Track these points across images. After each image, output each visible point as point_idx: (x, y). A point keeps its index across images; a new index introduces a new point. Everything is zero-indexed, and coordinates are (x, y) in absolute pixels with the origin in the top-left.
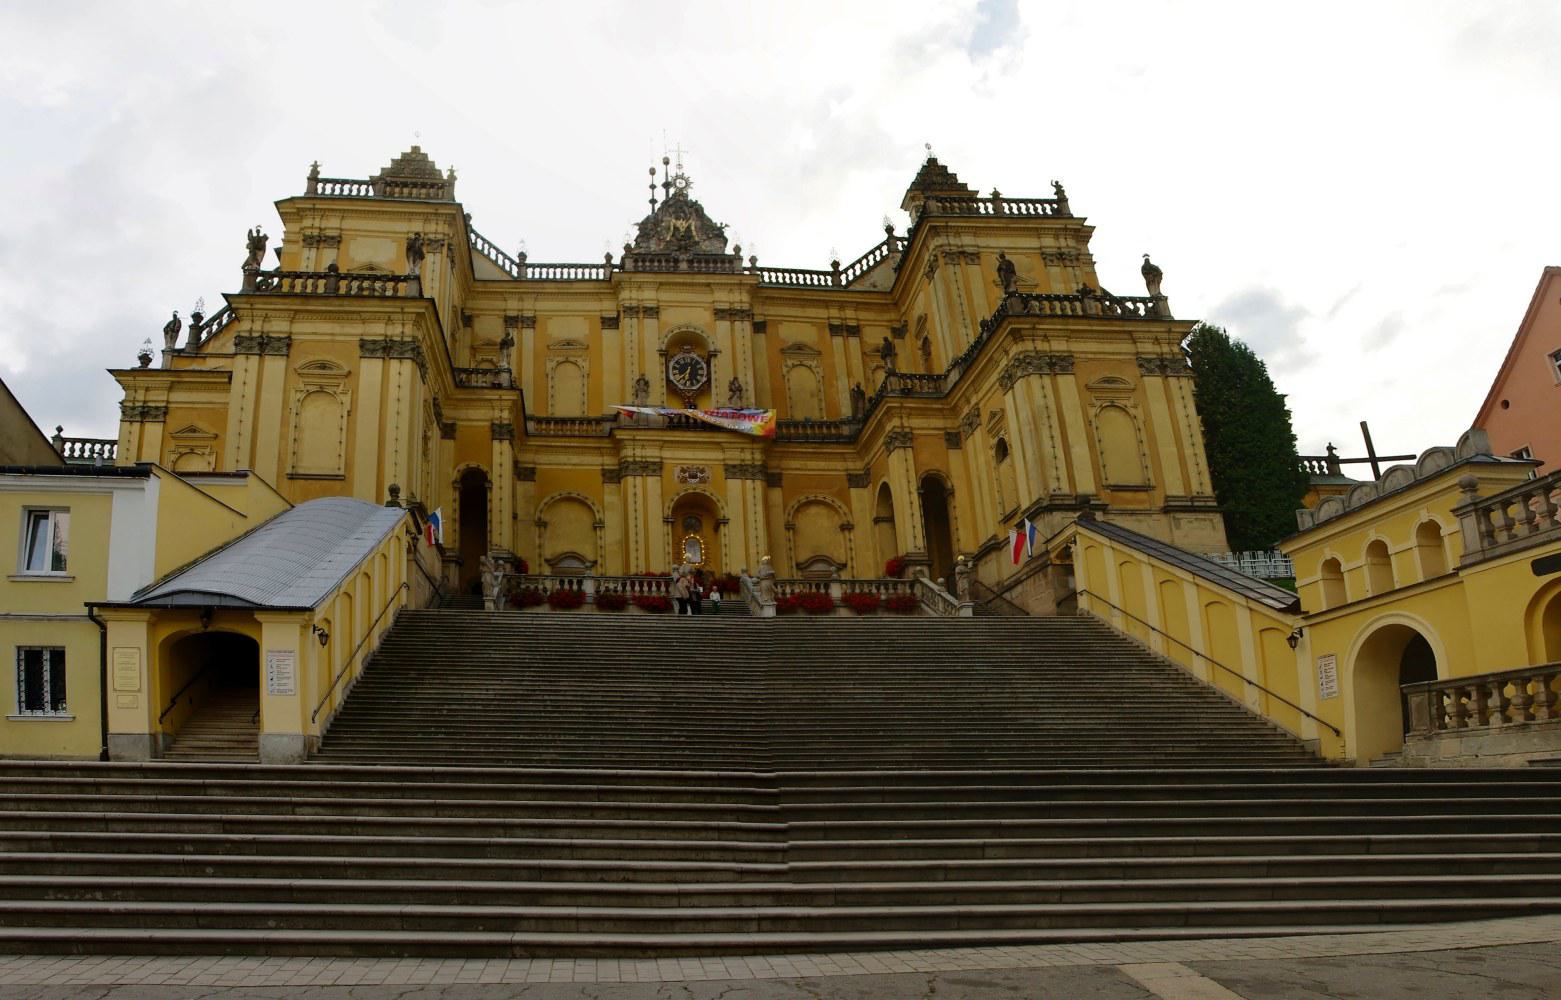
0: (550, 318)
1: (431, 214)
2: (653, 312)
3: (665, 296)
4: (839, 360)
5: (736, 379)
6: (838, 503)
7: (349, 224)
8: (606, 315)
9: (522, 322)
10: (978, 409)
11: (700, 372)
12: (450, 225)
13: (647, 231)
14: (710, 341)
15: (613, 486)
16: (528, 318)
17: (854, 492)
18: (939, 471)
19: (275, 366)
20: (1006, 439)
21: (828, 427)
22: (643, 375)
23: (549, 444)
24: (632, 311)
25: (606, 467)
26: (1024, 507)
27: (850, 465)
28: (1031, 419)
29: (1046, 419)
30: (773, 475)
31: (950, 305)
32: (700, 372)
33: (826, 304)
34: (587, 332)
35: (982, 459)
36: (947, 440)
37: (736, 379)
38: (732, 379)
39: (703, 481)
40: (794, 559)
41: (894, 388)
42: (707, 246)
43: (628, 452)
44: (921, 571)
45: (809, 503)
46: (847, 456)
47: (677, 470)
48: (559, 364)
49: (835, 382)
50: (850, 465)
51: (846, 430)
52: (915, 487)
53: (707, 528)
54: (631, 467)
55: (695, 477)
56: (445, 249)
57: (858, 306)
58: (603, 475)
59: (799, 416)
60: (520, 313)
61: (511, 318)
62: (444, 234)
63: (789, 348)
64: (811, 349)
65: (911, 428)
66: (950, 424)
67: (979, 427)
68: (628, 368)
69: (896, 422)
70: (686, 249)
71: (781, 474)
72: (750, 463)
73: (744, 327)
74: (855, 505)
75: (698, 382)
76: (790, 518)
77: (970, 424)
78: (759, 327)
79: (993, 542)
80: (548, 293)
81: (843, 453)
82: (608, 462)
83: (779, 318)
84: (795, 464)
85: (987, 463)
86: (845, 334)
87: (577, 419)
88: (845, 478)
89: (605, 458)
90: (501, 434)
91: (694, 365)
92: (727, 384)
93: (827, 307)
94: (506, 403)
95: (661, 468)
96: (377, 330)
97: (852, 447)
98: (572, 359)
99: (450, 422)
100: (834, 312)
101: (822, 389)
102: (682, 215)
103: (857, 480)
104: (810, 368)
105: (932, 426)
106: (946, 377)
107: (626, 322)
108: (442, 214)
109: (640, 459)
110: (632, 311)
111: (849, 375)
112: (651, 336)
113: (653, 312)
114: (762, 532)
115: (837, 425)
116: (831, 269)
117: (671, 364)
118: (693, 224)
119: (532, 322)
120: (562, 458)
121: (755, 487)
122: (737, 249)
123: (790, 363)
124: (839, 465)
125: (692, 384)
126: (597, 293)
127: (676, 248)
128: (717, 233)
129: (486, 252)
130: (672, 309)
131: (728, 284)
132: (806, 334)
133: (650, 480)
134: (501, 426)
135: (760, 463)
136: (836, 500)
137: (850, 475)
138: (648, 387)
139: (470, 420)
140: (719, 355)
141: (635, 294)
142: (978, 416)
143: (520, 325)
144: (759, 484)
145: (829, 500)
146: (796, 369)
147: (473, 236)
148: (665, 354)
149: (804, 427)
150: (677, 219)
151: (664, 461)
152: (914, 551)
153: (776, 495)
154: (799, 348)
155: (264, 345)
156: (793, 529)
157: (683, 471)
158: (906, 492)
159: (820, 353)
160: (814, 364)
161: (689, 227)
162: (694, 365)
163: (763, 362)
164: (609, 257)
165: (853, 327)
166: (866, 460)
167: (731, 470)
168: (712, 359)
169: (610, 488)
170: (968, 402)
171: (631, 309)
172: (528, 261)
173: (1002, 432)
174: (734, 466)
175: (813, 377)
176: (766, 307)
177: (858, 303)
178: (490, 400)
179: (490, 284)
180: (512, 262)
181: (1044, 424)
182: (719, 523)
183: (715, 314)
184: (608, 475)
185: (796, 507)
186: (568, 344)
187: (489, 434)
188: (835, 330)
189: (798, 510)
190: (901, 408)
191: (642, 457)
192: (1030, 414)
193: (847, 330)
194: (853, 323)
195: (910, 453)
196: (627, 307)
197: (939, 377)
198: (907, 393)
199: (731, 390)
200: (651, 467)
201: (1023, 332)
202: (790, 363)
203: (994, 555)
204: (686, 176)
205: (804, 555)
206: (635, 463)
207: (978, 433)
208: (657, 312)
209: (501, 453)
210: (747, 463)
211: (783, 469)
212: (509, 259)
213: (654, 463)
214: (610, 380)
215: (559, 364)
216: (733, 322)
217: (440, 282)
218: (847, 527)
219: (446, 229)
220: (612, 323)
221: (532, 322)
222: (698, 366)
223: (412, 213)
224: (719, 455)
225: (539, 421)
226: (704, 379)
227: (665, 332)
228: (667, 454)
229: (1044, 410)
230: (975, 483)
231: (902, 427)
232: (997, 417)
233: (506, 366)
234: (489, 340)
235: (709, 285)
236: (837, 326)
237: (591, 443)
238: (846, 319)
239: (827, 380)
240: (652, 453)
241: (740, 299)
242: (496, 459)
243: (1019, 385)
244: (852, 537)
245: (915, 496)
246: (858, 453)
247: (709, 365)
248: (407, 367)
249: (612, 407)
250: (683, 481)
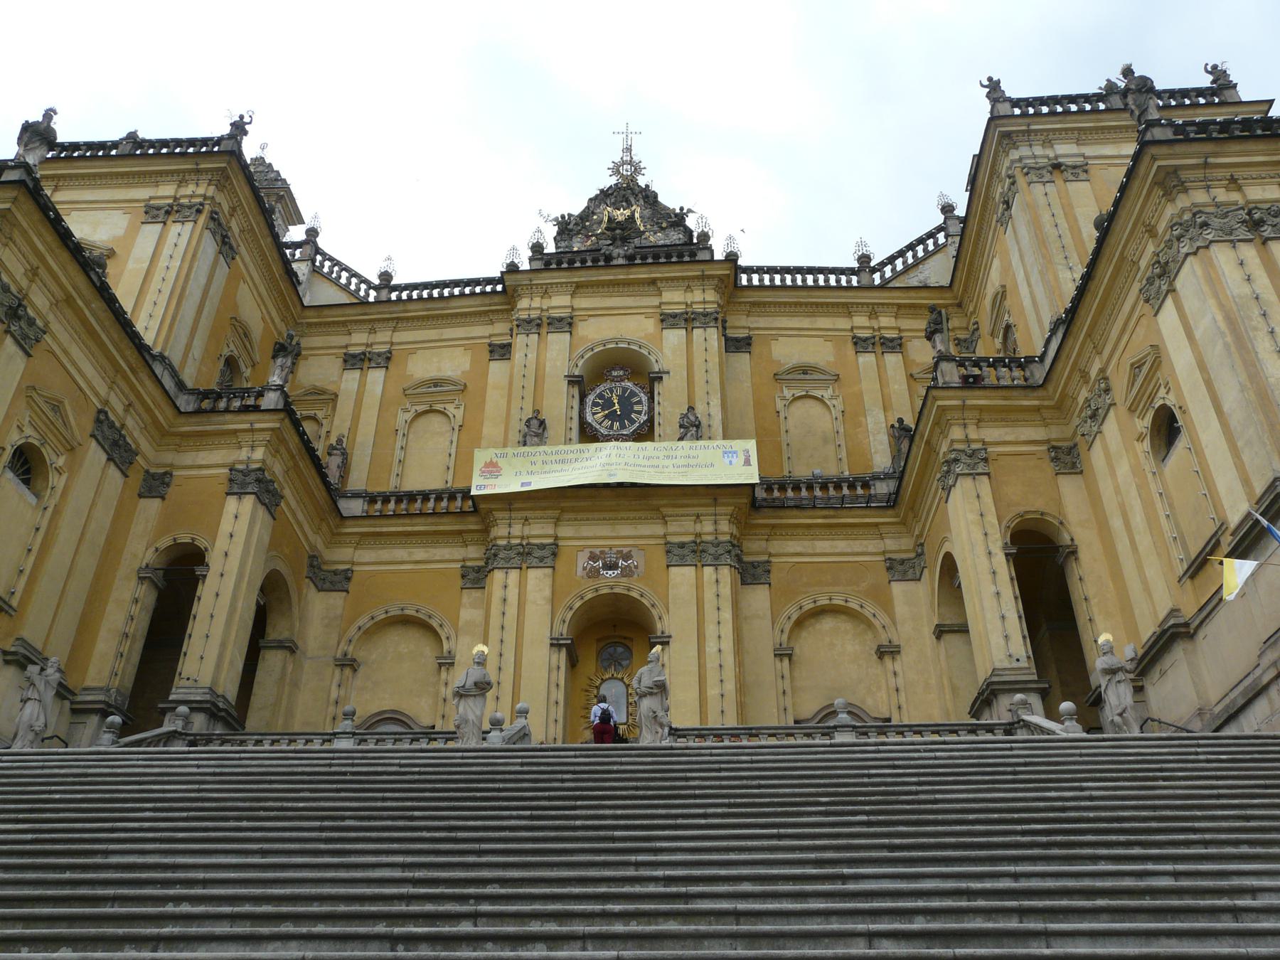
0: (413, 352)
1: (190, 171)
4: (869, 387)
5: (691, 409)
6: (869, 610)
8: (497, 341)
9: (370, 360)
10: (1106, 379)
11: (636, 408)
12: (220, 188)
13: (571, 227)
14: (653, 359)
15: (476, 594)
16: (379, 355)
17: (898, 589)
18: (1042, 514)
20: (1171, 401)
21: (852, 486)
22: (538, 412)
23: (378, 530)
25: (469, 564)
26: (1234, 519)
27: (890, 544)
28: (1222, 325)
29: (1261, 319)
30: (754, 565)
31: (1041, 241)
32: (636, 408)
33: (847, 310)
34: (467, 366)
35: (1123, 469)
36: (1053, 460)
37: (691, 409)
38: (685, 412)
39: (627, 572)
40: (790, 710)
41: (947, 379)
42: (656, 238)
43: (500, 531)
44: (1024, 703)
45: (819, 612)
46: (884, 529)
47: (582, 560)
48: (419, 415)
49: (863, 419)
50: (890, 544)
51: (882, 488)
52: (1000, 544)
54: (502, 555)
55: (613, 566)
56: (202, 219)
57: (900, 310)
58: (463, 576)
60: (368, 349)
61: (354, 356)
62: (205, 197)
63: (789, 371)
64: (823, 372)
65: (984, 443)
66: (1054, 433)
67: (1112, 413)
68: (516, 404)
69: (956, 433)
70: (625, 240)
71: (769, 562)
72: (709, 538)
73: (709, 339)
74: (901, 609)
75: (632, 422)
76: (785, 636)
77: (1093, 416)
78: (736, 345)
79: (1172, 622)
80: (413, 318)
81: (876, 525)
82: (471, 556)
83: (773, 332)
84: (793, 546)
85: (1137, 471)
86: (879, 349)
87: (431, 492)
88: (883, 566)
89: (471, 548)
90: (244, 485)
92: (677, 419)
93: (850, 315)
94: (259, 436)
95: (554, 554)
97: (890, 512)
98: (439, 407)
99: (161, 471)
100: (861, 320)
101: (841, 430)
102: (624, 204)
103: (900, 568)
104: (820, 400)
105: (1023, 438)
106: (1042, 358)
107: (520, 341)
108: (207, 171)
109: (518, 541)
110: (534, 325)
111: (885, 409)
113: (566, 324)
114: (729, 660)
116: (855, 265)
117: (590, 398)
120: (400, 553)
121: (719, 579)
122: (704, 237)
123: (788, 393)
124: (872, 545)
125: (623, 427)
126: (486, 313)
127: (610, 242)
128: (677, 220)
129: (334, 275)
130: (592, 320)
131: (683, 278)
132: (817, 352)
133: (532, 574)
134: (245, 473)
135: (727, 538)
136: (866, 604)
137: (890, 559)
138: (544, 429)
139: (201, 467)
140: (664, 376)
141: (537, 302)
142: (1107, 391)
143: (366, 364)
144: (725, 573)
145: (853, 605)
146: (799, 404)
147: (319, 258)
148: (580, 384)
149: (810, 487)
151: (561, 543)
152: (1006, 664)
154: (805, 370)
156: (790, 656)
157: (593, 558)
158: (981, 550)
159: (837, 378)
160: (827, 394)
161: (632, 217)
162: (626, 401)
163: (743, 391)
165: (892, 340)
166: (917, 533)
167: (677, 551)
168: (656, 384)
169: (469, 597)
170: (1085, 375)
171: (529, 321)
172: (393, 283)
173: (1162, 392)
174: (682, 545)
175: (827, 413)
176: (751, 319)
177: (899, 306)
178: (235, 432)
179: (326, 312)
180: (370, 286)
181: (1255, 329)
183: (662, 321)
184: (472, 576)
185: (794, 617)
186: (435, 386)
187: (225, 488)
188: (861, 344)
189: (799, 624)
190: (963, 407)
191: (522, 538)
192: (1219, 318)
193: (882, 344)
195: (984, 485)
196: (524, 320)
197: (1030, 360)
198: (971, 383)
199: (681, 426)
200: (538, 553)
201: (1184, 175)
202: (788, 393)
203: (1179, 652)
204: (636, 159)
206: (509, 547)
207: (1111, 427)
208: (570, 324)
209: (236, 517)
210: (706, 538)
211: (770, 555)
212: (366, 281)
213: (542, 547)
215: (419, 415)
216: (689, 332)
217: (183, 261)
218: (887, 652)
219: (211, 191)
221: (386, 359)
222: (635, 399)
223: (160, 173)
225: (372, 499)
226: (644, 418)
227: (580, 350)
229: (1253, 303)
230: (1116, 523)
231: (968, 441)
232: (1145, 369)
233: (279, 382)
234: (315, 387)
235: (653, 282)
236: (865, 340)
237: (447, 525)
238: (880, 329)
239: (852, 415)
241: (704, 298)
242: (226, 525)
243: (1189, 278)
244: (898, 667)
245: (1000, 559)
246: (903, 523)
247: (651, 399)
250: (593, 574)
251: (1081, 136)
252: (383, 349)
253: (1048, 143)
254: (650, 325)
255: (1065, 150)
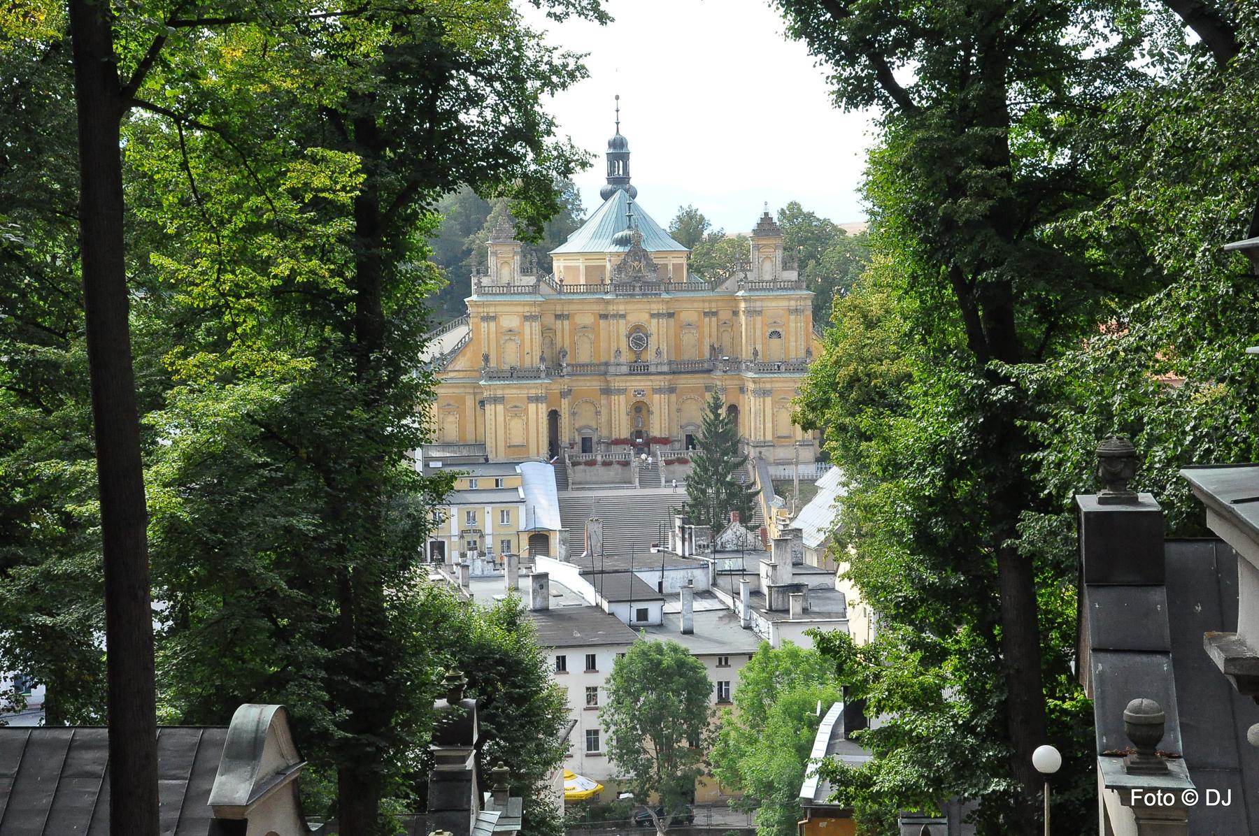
2: (623, 316)
3: (629, 307)
4: (706, 329)
7: (499, 309)
8: (602, 312)
19: (500, 408)
24: (614, 316)
33: (703, 301)
39: (643, 395)
51: (706, 366)
53: (644, 411)
59: (686, 357)
68: (612, 344)
73: (663, 321)
78: (671, 315)
84: (682, 382)
91: (640, 339)
96: (533, 392)
100: (707, 305)
112: (622, 328)
113: (623, 316)
115: (702, 362)
118: (643, 263)
119: (567, 317)
150: (636, 260)
153: (673, 397)
155: (496, 400)
163: (672, 332)
164: (602, 281)
169: (603, 397)
182: (649, 412)
188: (706, 314)
194: (714, 310)
205: (684, 422)
214: (603, 345)
220: (604, 317)
221: (567, 317)
224: (650, 383)
228: (628, 384)
239: (700, 340)
240: (622, 385)
248: (544, 406)
249: (603, 360)
250: (635, 396)
251: (762, 300)
252: (567, 313)
253: (755, 300)
254: (647, 316)
255: (758, 304)
